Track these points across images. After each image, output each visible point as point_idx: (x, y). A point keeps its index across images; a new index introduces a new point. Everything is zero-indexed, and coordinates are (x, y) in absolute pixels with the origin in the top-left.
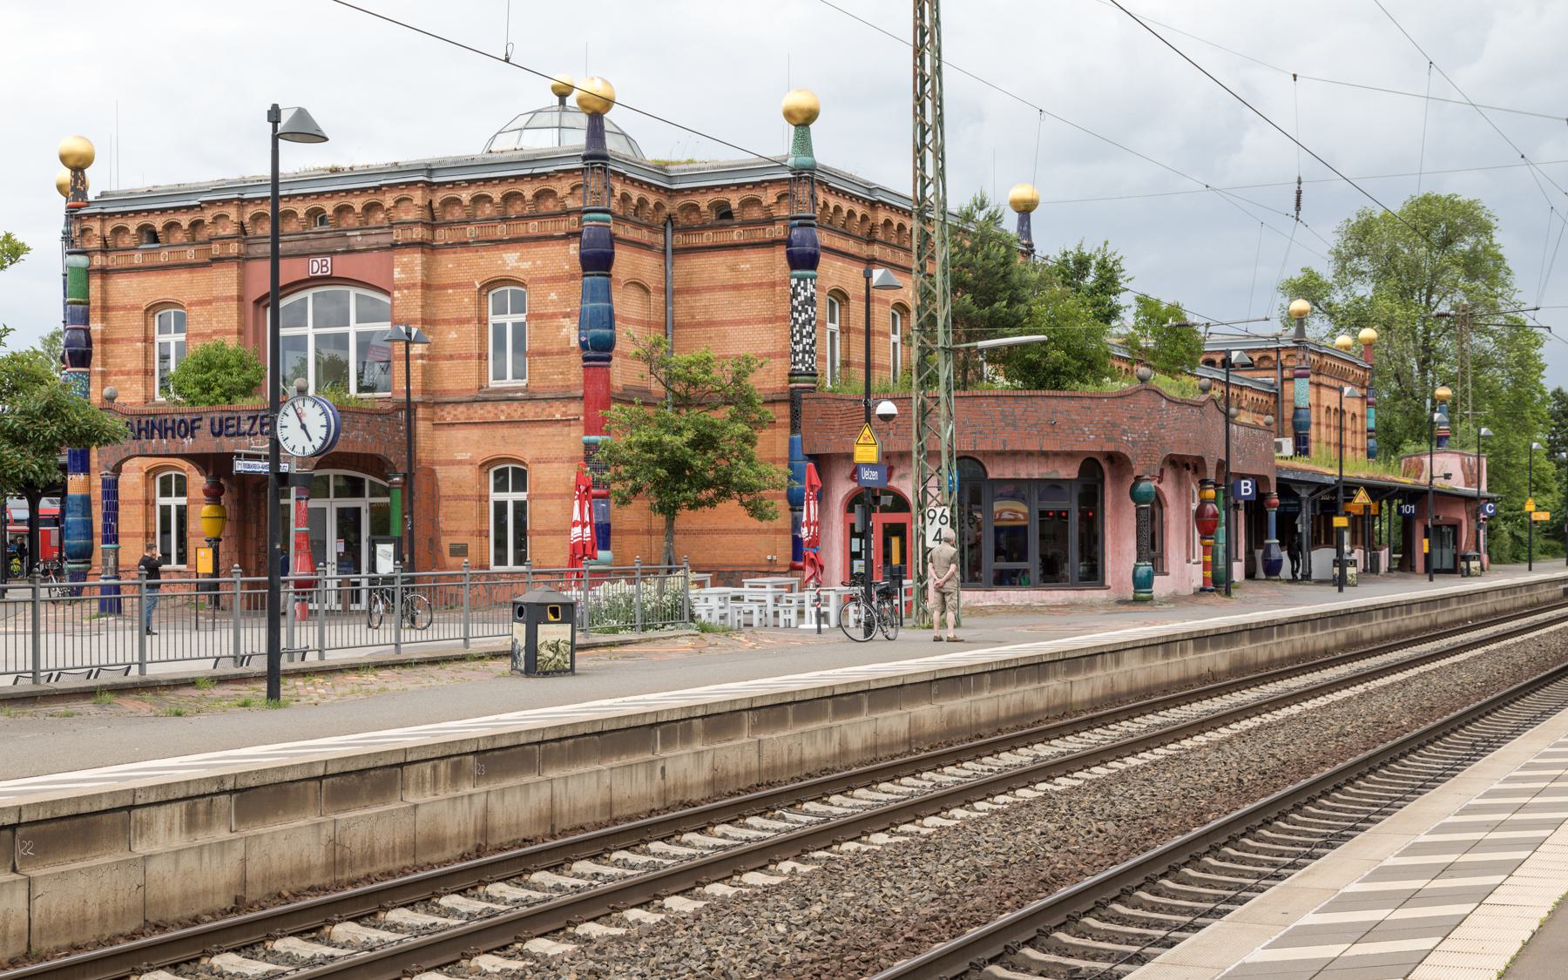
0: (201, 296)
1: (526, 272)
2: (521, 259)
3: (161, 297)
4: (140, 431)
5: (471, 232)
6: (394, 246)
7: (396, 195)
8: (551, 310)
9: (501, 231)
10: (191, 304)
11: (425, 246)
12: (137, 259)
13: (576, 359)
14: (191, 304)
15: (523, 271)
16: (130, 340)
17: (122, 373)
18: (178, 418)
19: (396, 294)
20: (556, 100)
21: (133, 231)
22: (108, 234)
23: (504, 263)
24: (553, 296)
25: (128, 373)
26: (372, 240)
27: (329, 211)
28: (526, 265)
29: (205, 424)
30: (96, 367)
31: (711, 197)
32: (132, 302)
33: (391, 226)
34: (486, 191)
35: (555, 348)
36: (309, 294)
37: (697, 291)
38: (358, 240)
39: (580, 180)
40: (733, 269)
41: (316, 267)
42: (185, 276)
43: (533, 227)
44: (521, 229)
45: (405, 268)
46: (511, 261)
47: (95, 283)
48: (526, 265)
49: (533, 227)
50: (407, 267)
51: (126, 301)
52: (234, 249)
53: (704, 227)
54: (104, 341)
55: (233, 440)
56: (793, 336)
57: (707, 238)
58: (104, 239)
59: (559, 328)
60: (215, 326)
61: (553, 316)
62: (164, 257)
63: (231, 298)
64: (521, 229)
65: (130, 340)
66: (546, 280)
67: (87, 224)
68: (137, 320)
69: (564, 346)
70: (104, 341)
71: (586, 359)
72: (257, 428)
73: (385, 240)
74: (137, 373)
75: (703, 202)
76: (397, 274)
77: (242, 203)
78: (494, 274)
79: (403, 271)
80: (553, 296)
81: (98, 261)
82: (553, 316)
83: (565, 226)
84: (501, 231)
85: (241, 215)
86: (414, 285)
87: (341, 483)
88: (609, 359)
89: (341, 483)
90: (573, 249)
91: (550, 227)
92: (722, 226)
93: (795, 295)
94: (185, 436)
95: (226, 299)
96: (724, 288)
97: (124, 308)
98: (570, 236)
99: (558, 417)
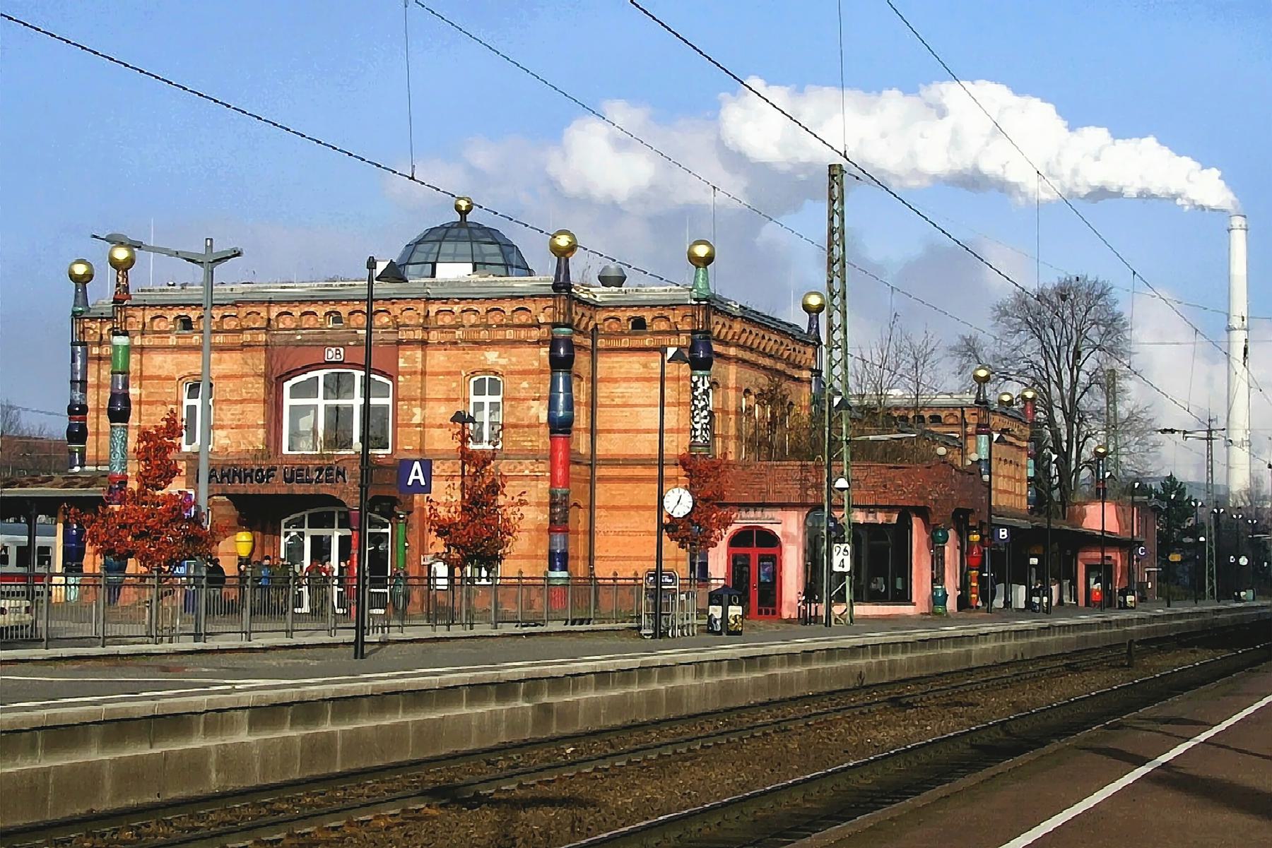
1: (504, 366)
2: (499, 357)
4: (222, 477)
7: (404, 306)
8: (523, 394)
9: (484, 335)
11: (424, 343)
12: (172, 340)
13: (545, 431)
19: (400, 378)
20: (457, 217)
21: (170, 319)
22: (147, 320)
27: (344, 315)
28: (503, 361)
29: (279, 474)
31: (630, 313)
33: (398, 327)
35: (526, 422)
36: (320, 374)
37: (615, 381)
39: (551, 303)
40: (645, 366)
41: (331, 355)
43: (510, 334)
44: (499, 335)
46: (492, 357)
47: (134, 358)
49: (510, 334)
52: (262, 337)
53: (622, 334)
54: (140, 403)
56: (693, 418)
57: (625, 342)
58: (144, 324)
59: (529, 408)
60: (245, 396)
62: (196, 339)
69: (533, 421)
70: (140, 403)
71: (552, 432)
73: (392, 337)
75: (624, 315)
76: (401, 363)
80: (525, 385)
81: (138, 341)
83: (535, 334)
85: (268, 312)
86: (415, 373)
87: (343, 516)
88: (569, 432)
89: (343, 516)
90: (544, 352)
91: (523, 334)
92: (636, 334)
93: (695, 388)
96: (637, 380)
97: (159, 378)
99: (527, 472)
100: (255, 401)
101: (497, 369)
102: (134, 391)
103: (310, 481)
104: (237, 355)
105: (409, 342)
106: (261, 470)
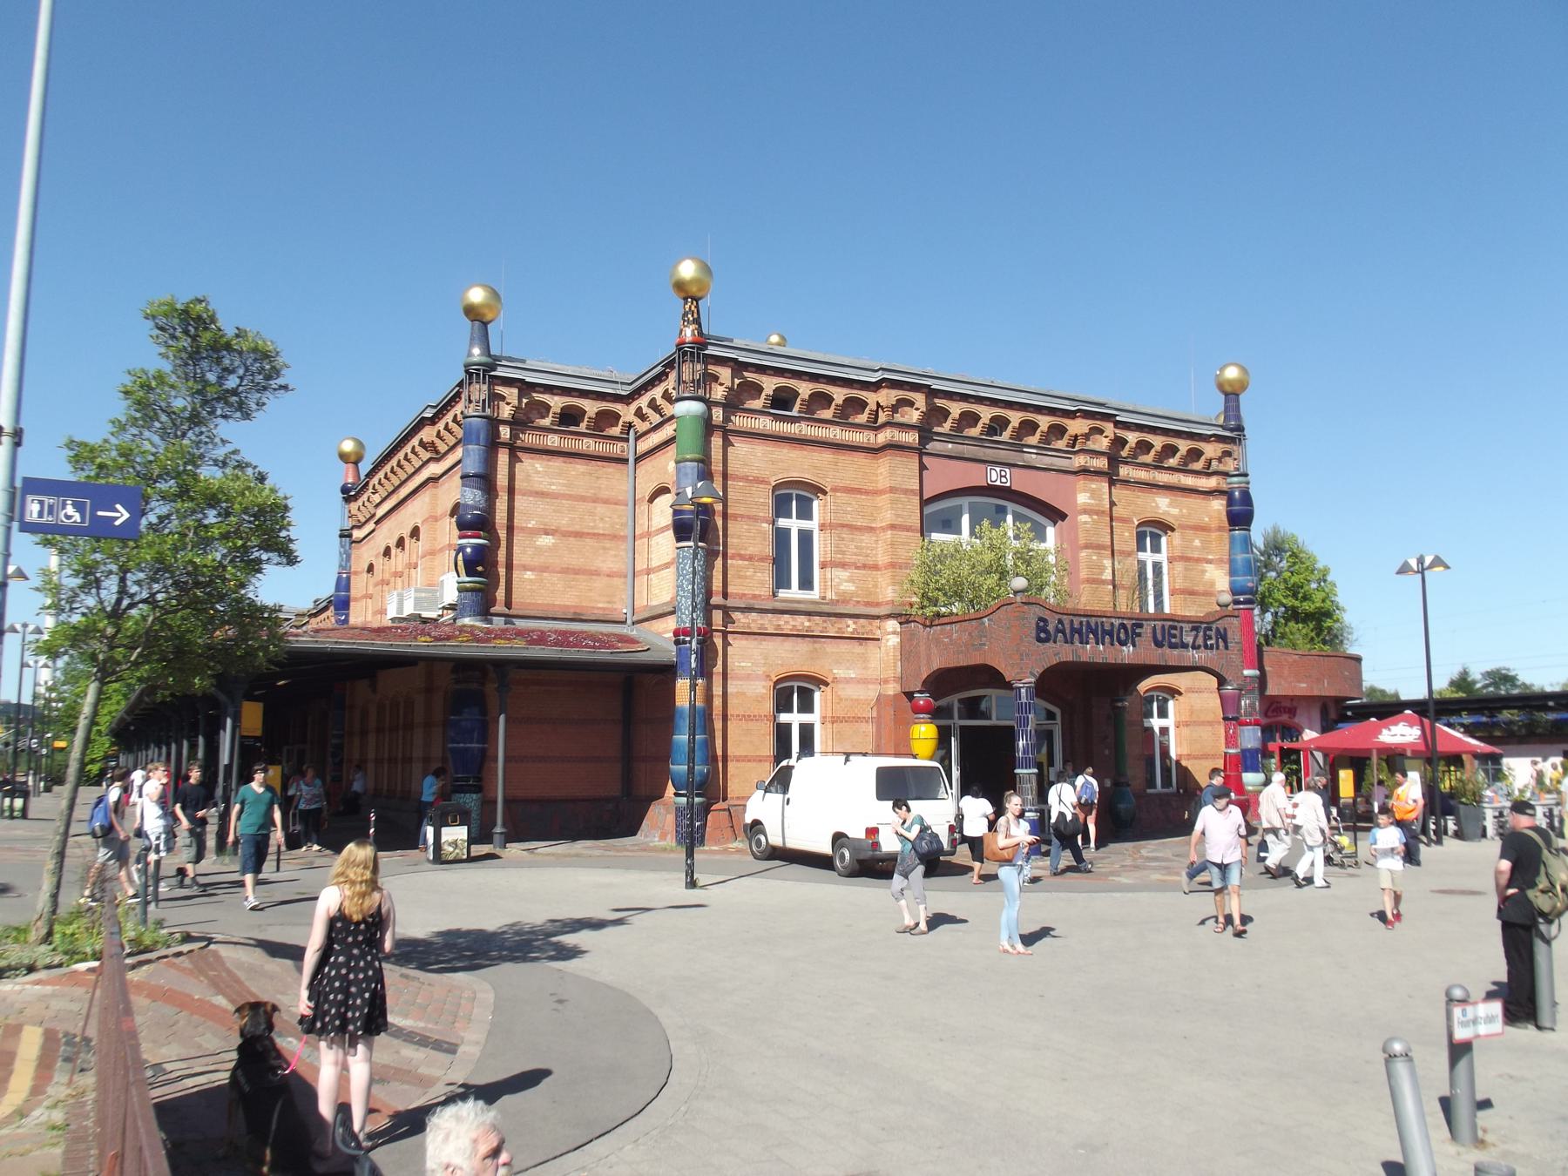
0: (847, 483)
2: (1170, 505)
3: (795, 475)
4: (1073, 630)
8: (1196, 555)
10: (835, 490)
14: (835, 490)
15: (1174, 516)
16: (754, 519)
17: (742, 557)
18: (1117, 622)
23: (1157, 507)
24: (1197, 543)
25: (750, 558)
28: (1175, 511)
29: (1147, 629)
32: (756, 473)
34: (1150, 438)
35: (1201, 588)
41: (995, 476)
42: (827, 456)
45: (1093, 494)
46: (1163, 506)
48: (1175, 511)
50: (1086, 495)
51: (745, 471)
55: (1176, 652)
61: (1198, 560)
65: (754, 519)
67: (712, 369)
68: (763, 500)
72: (1200, 641)
74: (762, 559)
76: (1083, 498)
77: (931, 393)
78: (1149, 515)
79: (1092, 497)
82: (1198, 560)
83: (1211, 483)
94: (1123, 643)
97: (745, 479)
103: (1185, 646)
106: (1123, 626)
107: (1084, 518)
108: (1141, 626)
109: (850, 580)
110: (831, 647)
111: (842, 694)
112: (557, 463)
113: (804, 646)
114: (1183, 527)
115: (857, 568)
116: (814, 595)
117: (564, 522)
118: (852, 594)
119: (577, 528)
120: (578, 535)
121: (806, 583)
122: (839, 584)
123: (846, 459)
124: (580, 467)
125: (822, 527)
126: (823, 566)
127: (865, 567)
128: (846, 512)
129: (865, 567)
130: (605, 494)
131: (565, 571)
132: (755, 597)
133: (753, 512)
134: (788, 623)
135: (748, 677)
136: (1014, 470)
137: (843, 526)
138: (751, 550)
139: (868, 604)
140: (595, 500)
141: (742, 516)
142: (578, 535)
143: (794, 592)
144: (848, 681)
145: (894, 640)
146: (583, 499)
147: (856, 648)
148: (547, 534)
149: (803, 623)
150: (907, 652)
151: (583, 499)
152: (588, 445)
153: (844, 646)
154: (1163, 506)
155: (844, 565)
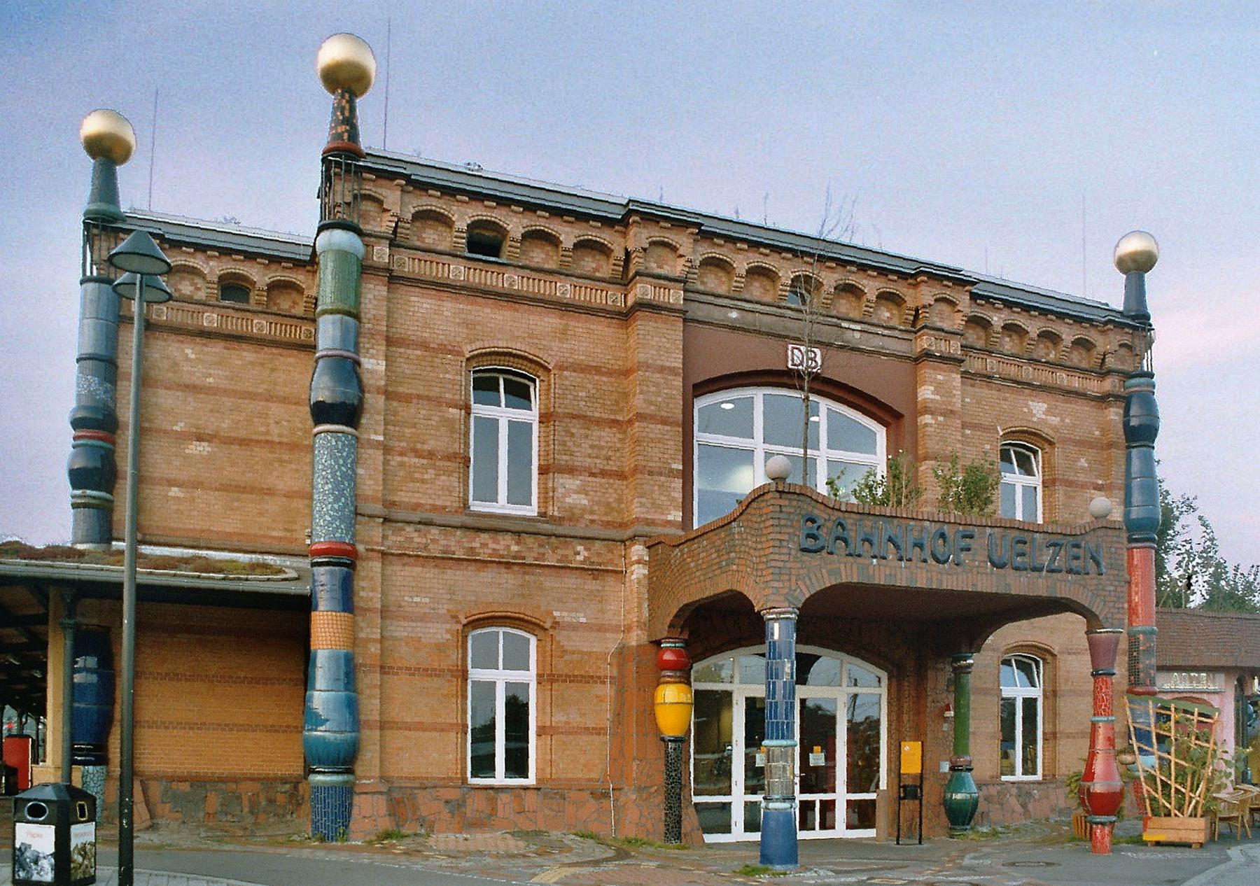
1: (1054, 428)
5: (992, 365)
6: (927, 355)
8: (1081, 478)
9: (1028, 373)
14: (561, 368)
17: (418, 454)
18: (933, 528)
23: (1031, 411)
24: (1083, 462)
25: (431, 455)
26: (876, 342)
28: (1055, 420)
30: (373, 429)
36: (758, 396)
38: (855, 335)
41: (797, 357)
43: (1063, 379)
44: (1044, 376)
45: (939, 387)
46: (1038, 411)
48: (1055, 420)
49: (1063, 379)
54: (389, 395)
63: (672, 371)
64: (1044, 376)
66: (1078, 443)
79: (936, 392)
84: (1028, 373)
90: (1114, 414)
95: (661, 369)
98: (1103, 400)
100: (664, 422)
101: (1047, 432)
102: (373, 365)
104: (603, 329)
105: (946, 359)
106: (943, 536)
107: (927, 419)
108: (972, 537)
109: (583, 491)
110: (549, 581)
111: (568, 645)
112: (217, 348)
113: (509, 580)
114: (1065, 441)
115: (592, 475)
116: (532, 511)
117: (225, 425)
118: (584, 510)
119: (242, 433)
120: (244, 442)
121: (519, 493)
122: (564, 496)
123: (579, 325)
124: (248, 354)
125: (545, 418)
126: (543, 471)
127: (604, 473)
128: (576, 398)
129: (604, 473)
130: (281, 390)
131: (225, 488)
132: (435, 508)
133: (435, 392)
134: (486, 545)
135: (423, 618)
136: (832, 352)
137: (574, 417)
138: (431, 445)
139: (607, 524)
140: (269, 398)
141: (419, 397)
142: (244, 442)
143: (502, 506)
144: (575, 627)
145: (639, 572)
146: (252, 396)
147: (591, 585)
148: (200, 439)
149: (508, 545)
150: (655, 587)
151: (252, 396)
152: (260, 326)
153: (571, 581)
154: (1038, 411)
155: (571, 471)
